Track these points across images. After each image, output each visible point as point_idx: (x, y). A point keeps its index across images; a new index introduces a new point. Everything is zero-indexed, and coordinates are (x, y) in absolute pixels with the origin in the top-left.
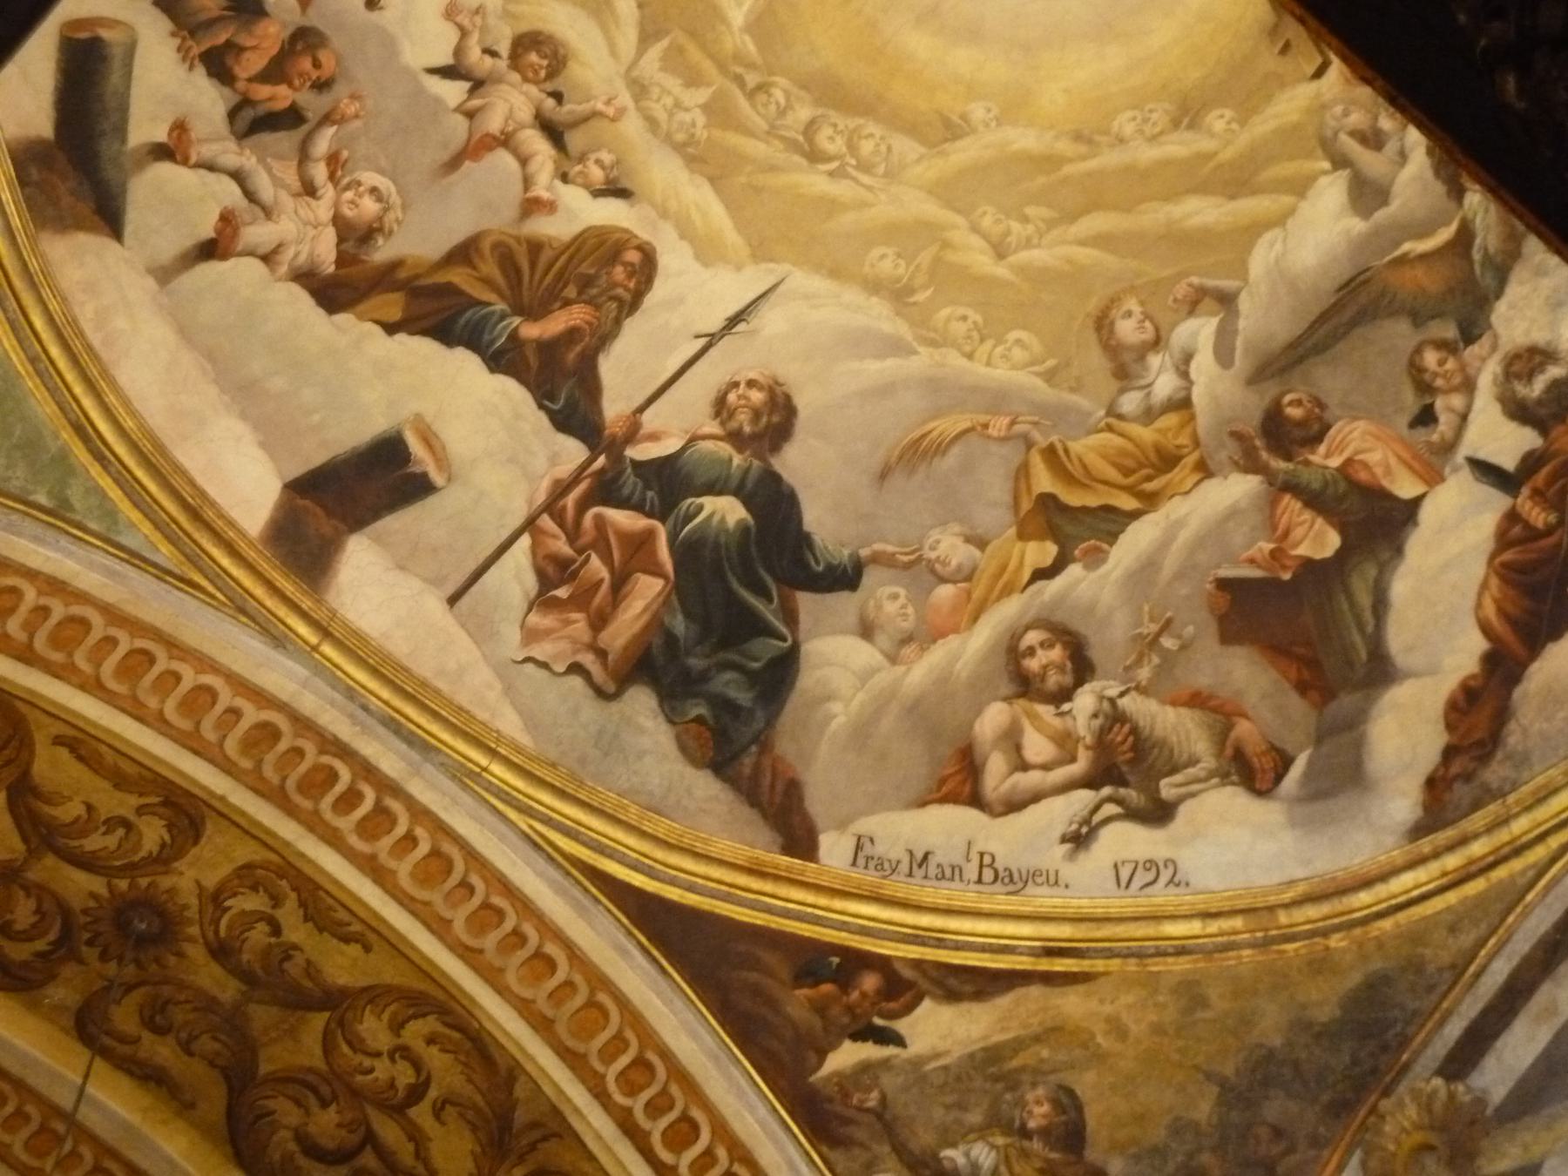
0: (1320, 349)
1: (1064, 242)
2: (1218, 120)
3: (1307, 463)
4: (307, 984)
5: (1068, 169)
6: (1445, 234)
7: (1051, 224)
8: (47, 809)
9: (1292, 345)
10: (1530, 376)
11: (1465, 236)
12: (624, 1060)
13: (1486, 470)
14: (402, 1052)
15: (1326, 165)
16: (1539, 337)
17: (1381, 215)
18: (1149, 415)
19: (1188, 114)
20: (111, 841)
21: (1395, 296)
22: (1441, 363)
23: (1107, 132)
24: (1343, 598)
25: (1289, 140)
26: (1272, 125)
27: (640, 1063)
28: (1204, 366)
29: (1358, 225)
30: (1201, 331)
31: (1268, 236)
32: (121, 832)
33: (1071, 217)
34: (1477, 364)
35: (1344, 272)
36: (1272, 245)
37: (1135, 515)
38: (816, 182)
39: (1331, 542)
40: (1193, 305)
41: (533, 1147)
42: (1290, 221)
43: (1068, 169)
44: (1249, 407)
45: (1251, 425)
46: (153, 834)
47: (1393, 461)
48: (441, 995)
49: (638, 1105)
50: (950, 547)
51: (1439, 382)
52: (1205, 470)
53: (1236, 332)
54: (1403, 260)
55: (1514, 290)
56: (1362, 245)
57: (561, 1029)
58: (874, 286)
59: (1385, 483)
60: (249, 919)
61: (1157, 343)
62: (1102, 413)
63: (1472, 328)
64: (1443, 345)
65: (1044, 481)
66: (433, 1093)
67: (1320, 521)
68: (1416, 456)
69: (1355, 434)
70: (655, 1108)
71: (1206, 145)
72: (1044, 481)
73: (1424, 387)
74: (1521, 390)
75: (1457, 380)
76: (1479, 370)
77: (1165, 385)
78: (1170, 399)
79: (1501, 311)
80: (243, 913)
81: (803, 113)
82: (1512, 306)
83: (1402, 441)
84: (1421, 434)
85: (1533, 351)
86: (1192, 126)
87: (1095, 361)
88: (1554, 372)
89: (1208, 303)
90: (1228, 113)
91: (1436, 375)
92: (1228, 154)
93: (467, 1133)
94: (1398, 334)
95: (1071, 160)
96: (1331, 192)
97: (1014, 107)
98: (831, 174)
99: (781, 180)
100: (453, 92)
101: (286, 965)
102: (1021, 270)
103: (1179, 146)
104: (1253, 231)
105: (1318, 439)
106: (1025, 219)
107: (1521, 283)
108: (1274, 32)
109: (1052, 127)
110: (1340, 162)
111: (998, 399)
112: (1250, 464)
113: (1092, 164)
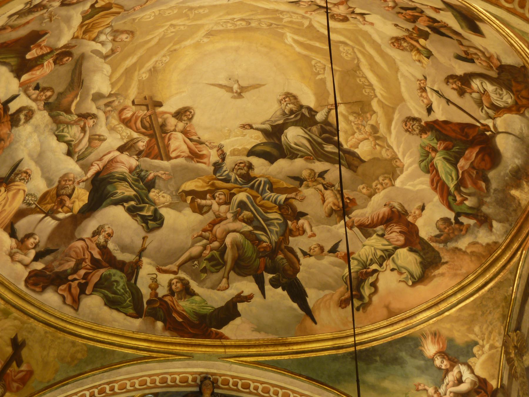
0: (74, 71)
1: (158, 35)
3: (52, 57)
5: (172, 44)
7: (164, 35)
9: (81, 65)
10: (26, 116)
11: (68, 111)
13: (13, 98)
15: (112, 92)
16: (33, 121)
17: (91, 97)
18: (101, 32)
19: (154, 71)
21: (70, 91)
22: (46, 96)
23: (169, 55)
24: (14, 56)
25: (126, 87)
26: (133, 85)
28: (98, 47)
29: (93, 91)
30: (105, 50)
33: (160, 40)
34: (38, 104)
36: (107, 72)
37: (82, 22)
38: (237, 16)
39: (28, 56)
40: (113, 51)
42: (109, 78)
43: (172, 44)
44: (77, 52)
45: (73, 50)
47: (34, 76)
51: (42, 93)
52: (75, 38)
53: (97, 56)
54: (76, 97)
56: (88, 90)
58: (200, 7)
59: (30, 73)
61: (114, 40)
62: (113, 25)
63: (48, 106)
64: (50, 97)
65: (114, 10)
67: (36, 56)
68: (30, 82)
69: (48, 70)
71: (143, 70)
73: (45, 89)
74: (25, 112)
75: (39, 98)
76: (37, 104)
77: (103, 38)
78: (99, 37)
79: (46, 113)
81: (254, 24)
82: (45, 116)
83: (36, 80)
84: (34, 85)
85: (31, 118)
86: (150, 70)
88: (23, 121)
89: (110, 53)
90: (144, 79)
91: (44, 93)
92: (136, 73)
94: (59, 89)
95: (172, 46)
97: (197, 45)
98: (235, 19)
99: (247, 14)
100: (358, 11)
102: (162, 27)
103: (149, 65)
104: (114, 70)
105: (55, 62)
106: (172, 32)
107: (47, 121)
108: (151, 98)
109: (184, 47)
110: (110, 95)
111: (143, 10)
112: (65, 46)
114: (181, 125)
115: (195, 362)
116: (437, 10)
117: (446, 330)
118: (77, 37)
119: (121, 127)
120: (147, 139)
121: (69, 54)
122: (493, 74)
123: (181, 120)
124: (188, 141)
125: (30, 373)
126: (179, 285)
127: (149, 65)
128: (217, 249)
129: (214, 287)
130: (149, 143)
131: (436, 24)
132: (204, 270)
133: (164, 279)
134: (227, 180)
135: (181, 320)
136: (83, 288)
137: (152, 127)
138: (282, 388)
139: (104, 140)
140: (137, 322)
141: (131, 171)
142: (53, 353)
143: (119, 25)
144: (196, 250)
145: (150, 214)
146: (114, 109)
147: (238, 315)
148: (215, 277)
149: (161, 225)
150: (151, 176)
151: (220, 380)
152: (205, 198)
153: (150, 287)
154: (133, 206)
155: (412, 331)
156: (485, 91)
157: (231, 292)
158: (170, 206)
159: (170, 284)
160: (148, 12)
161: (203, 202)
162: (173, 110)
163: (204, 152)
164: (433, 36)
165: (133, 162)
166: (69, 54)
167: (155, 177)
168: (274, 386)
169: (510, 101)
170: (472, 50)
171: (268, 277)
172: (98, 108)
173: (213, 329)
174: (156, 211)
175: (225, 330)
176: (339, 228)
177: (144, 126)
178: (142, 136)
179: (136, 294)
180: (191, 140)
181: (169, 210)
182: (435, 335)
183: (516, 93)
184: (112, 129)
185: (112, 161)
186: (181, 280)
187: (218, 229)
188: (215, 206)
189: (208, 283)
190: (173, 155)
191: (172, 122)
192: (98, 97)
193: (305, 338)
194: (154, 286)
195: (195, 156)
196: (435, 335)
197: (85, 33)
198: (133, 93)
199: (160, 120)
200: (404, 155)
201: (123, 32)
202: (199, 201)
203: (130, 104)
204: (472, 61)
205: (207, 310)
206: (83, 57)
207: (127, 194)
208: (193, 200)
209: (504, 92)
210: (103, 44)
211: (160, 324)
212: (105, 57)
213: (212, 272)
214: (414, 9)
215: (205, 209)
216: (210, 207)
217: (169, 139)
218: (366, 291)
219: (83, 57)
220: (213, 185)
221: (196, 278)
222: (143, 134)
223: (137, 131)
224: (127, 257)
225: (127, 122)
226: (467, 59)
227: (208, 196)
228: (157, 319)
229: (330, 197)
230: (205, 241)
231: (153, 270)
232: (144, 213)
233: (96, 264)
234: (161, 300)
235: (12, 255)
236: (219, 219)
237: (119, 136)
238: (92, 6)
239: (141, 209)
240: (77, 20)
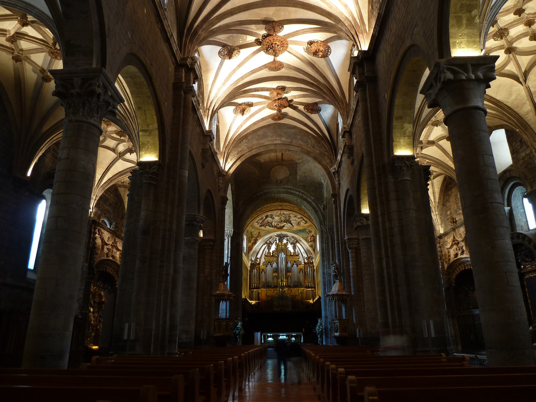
117: (309, 229)
125: (261, 235)
133: (275, 224)
136: (266, 226)
142: (264, 232)
144: (279, 220)
157: (284, 224)
171: (288, 223)
176: (296, 218)
179: (272, 225)
182: (308, 229)
194: (274, 224)
196: (308, 229)
218: (300, 224)
221: (279, 223)
229: (294, 215)
233: (267, 223)
235: (257, 225)
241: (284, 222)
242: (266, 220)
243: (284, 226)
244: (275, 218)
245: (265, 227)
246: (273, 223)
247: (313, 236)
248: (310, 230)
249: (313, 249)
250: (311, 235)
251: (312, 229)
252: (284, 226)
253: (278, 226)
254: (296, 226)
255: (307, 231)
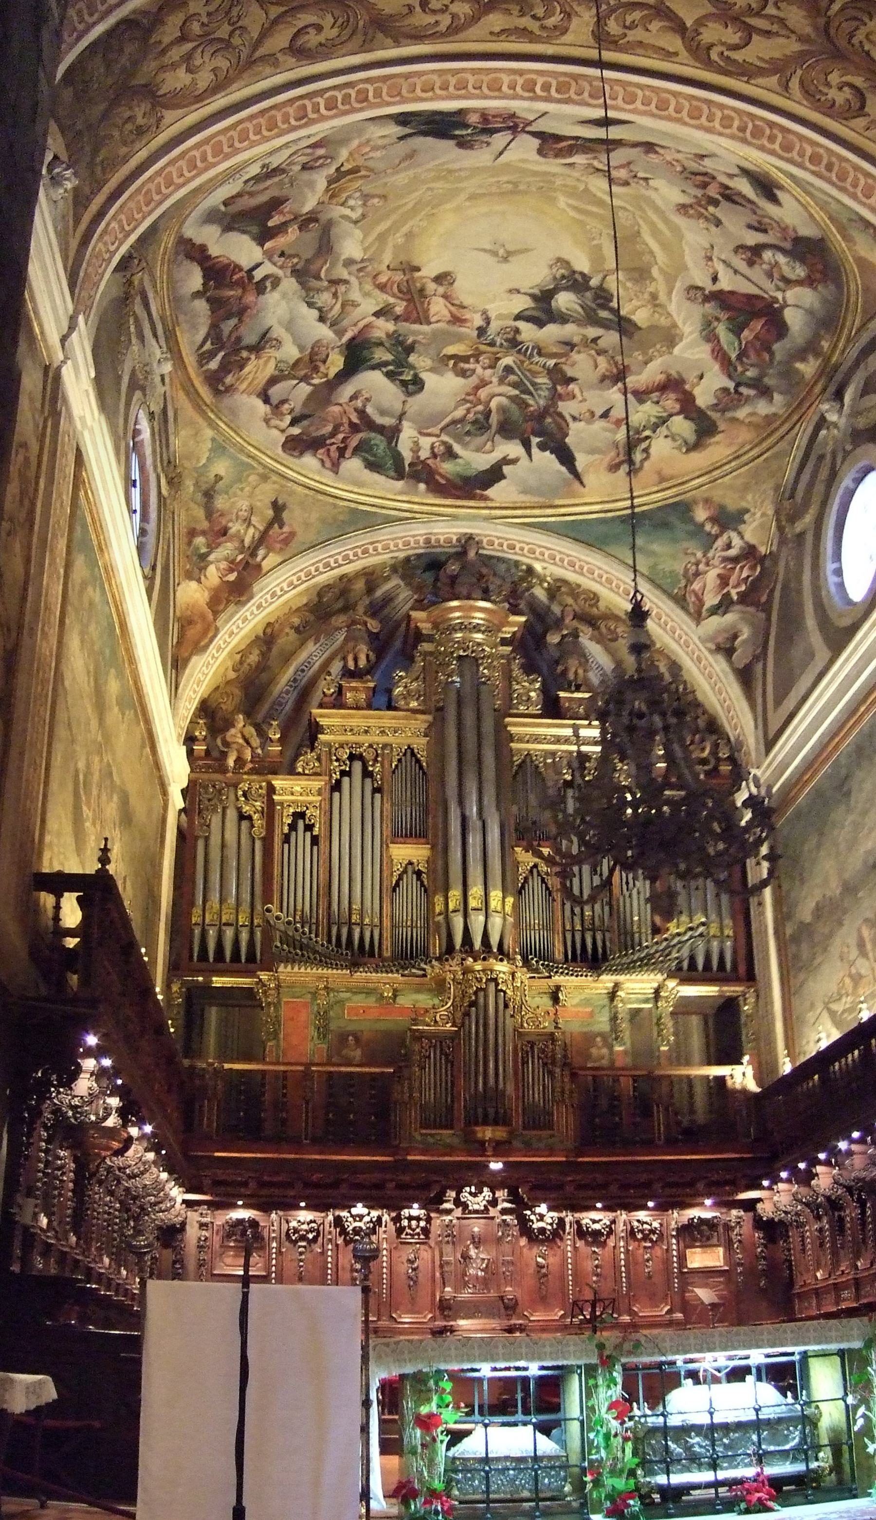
0: (321, 239)
2: (400, 241)
4: (505, 6)
6: (323, 275)
8: (662, 24)
12: (371, 94)
14: (445, 9)
19: (409, 236)
20: (629, 19)
25: (381, 250)
27: (366, 99)
28: (347, 212)
29: (343, 257)
30: (354, 215)
31: (362, 237)
32: (628, 23)
35: (336, 248)
40: (364, 216)
41: (365, 34)
44: (324, 217)
45: (319, 216)
46: (613, 27)
48: (451, 39)
49: (353, 93)
50: (378, 154)
55: (296, 284)
57: (402, 80)
60: (549, 14)
61: (364, 205)
65: (363, 173)
66: (418, 9)
70: (347, 99)
71: (398, 235)
72: (363, 173)
77: (351, 202)
80: (554, 15)
87: (379, 191)
92: (390, 239)
93: (393, 12)
96: (358, 255)
101: (518, 8)
103: (405, 229)
108: (408, 263)
110: (362, 261)
113: (423, 213)
114: (441, 290)
115: (459, 523)
116: (731, 176)
118: (323, 203)
119: (377, 292)
120: (405, 303)
121: (316, 220)
122: (788, 245)
123: (441, 284)
124: (449, 305)
126: (442, 448)
127: (405, 229)
128: (481, 413)
129: (478, 450)
130: (406, 307)
131: (728, 192)
132: (468, 433)
133: (426, 442)
134: (492, 344)
135: (443, 482)
137: (409, 291)
138: (548, 549)
139: (359, 305)
140: (400, 484)
141: (388, 336)
143: (368, 189)
144: (459, 413)
145: (409, 378)
146: (368, 274)
147: (503, 477)
148: (480, 440)
149: (423, 388)
150: (410, 341)
151: (485, 540)
152: (468, 362)
153: (411, 450)
154: (392, 371)
155: (683, 497)
156: (777, 263)
158: (432, 370)
159: (432, 448)
160: (403, 175)
161: (467, 366)
162: (433, 274)
163: (467, 316)
164: (724, 204)
165: (390, 327)
166: (316, 220)
167: (414, 342)
168: (540, 546)
169: (803, 274)
170: (766, 220)
172: (349, 274)
173: (478, 491)
174: (416, 376)
175: (489, 492)
177: (400, 291)
178: (399, 301)
179: (398, 458)
180: (453, 305)
181: (429, 373)
183: (811, 268)
184: (367, 295)
185: (368, 326)
186: (444, 443)
187: (483, 394)
188: (479, 370)
189: (472, 446)
190: (433, 320)
191: (431, 286)
192: (349, 262)
193: (572, 501)
195: (456, 320)
197: (332, 197)
198: (387, 258)
199: (418, 285)
200: (684, 324)
201: (373, 196)
202: (462, 365)
203: (385, 268)
204: (765, 231)
205: (472, 472)
206: (330, 223)
207: (384, 359)
208: (455, 364)
209: (798, 264)
210: (352, 208)
211: (422, 486)
212: (356, 222)
213: (476, 435)
214: (705, 174)
215: (468, 373)
216: (474, 371)
217: (429, 304)
219: (330, 223)
220: (477, 348)
221: (458, 439)
222: (402, 299)
223: (394, 296)
224: (387, 421)
225: (382, 287)
226: (761, 228)
227: (472, 360)
228: (419, 481)
230: (468, 405)
231: (415, 433)
232: (403, 378)
234: (423, 462)
236: (483, 383)
237: (374, 302)
238: (338, 170)
239: (401, 373)
240: (321, 184)
241: (507, 430)
242: (347, 390)
243: (494, 475)
244: (429, 378)
245: (335, 467)
246: (408, 433)
247: (749, 552)
248: (732, 503)
249: (741, 666)
250: (733, 552)
251: (746, 488)
252: (494, 475)
253: (447, 468)
254: (607, 478)
255: (701, 514)
